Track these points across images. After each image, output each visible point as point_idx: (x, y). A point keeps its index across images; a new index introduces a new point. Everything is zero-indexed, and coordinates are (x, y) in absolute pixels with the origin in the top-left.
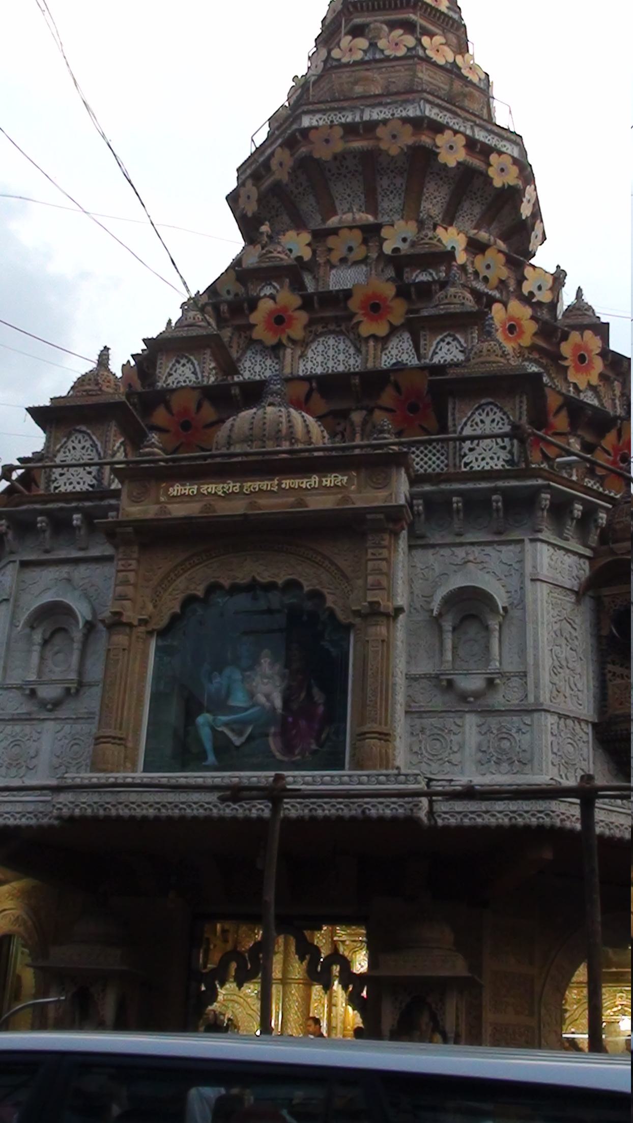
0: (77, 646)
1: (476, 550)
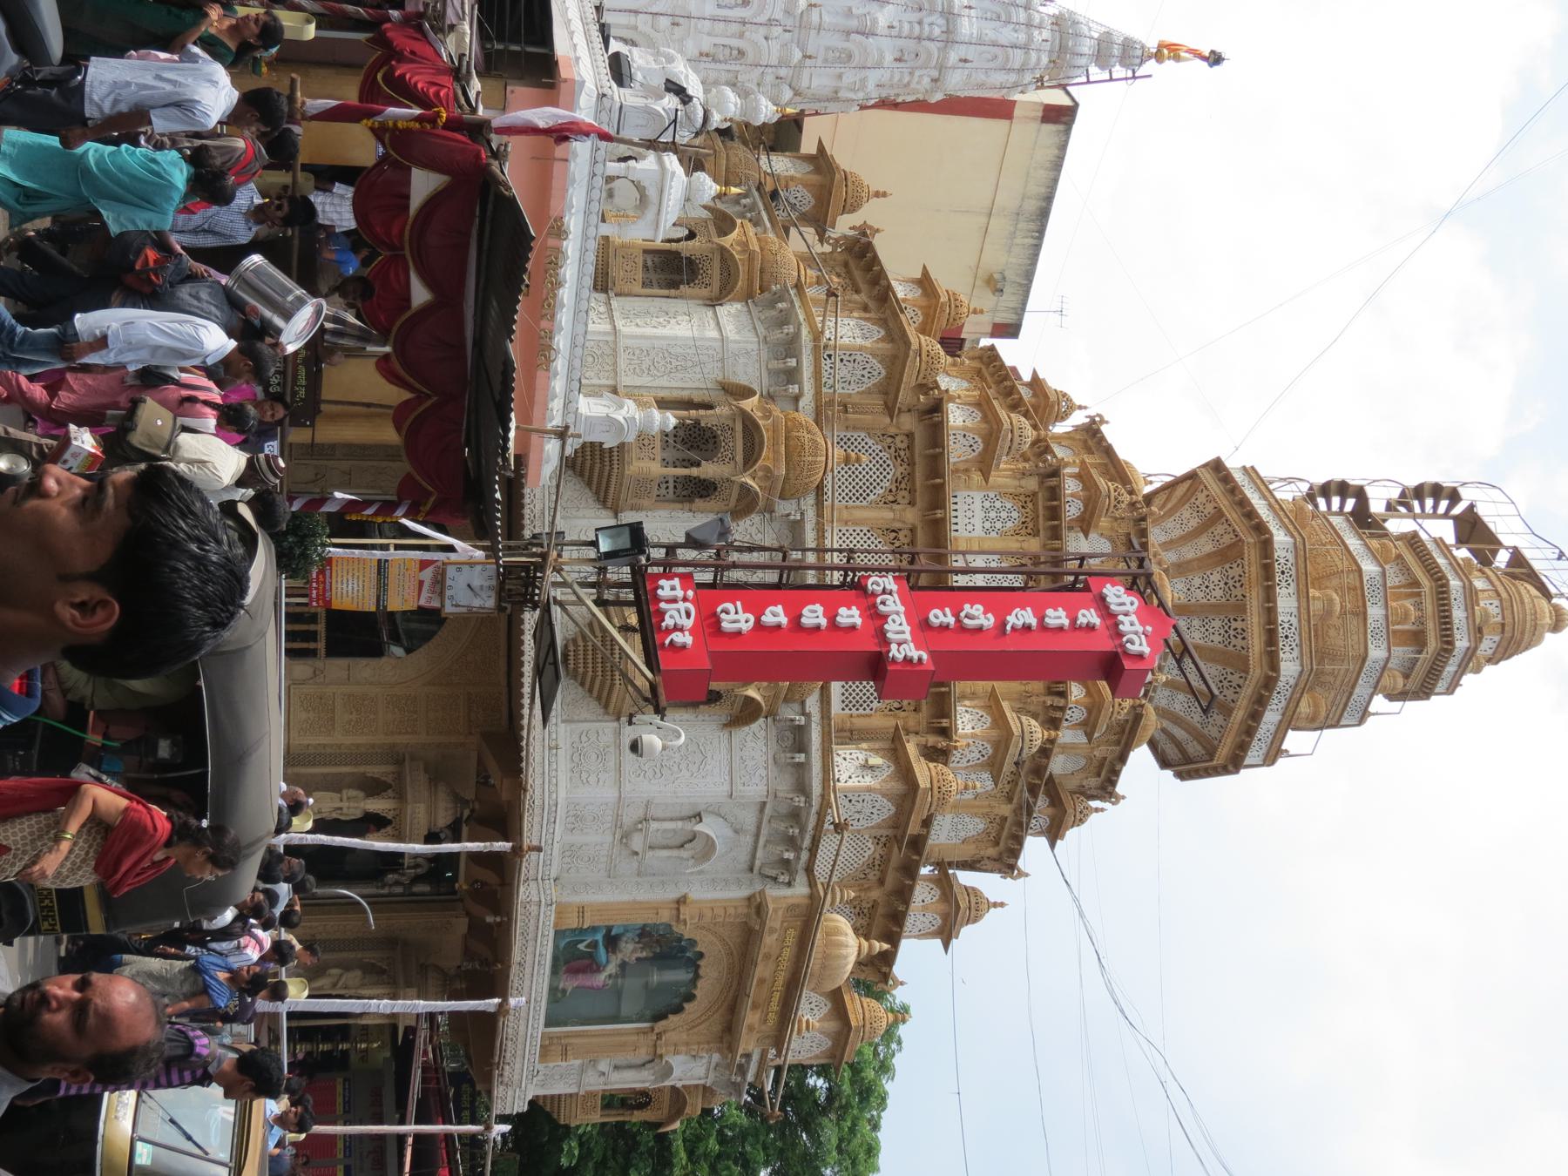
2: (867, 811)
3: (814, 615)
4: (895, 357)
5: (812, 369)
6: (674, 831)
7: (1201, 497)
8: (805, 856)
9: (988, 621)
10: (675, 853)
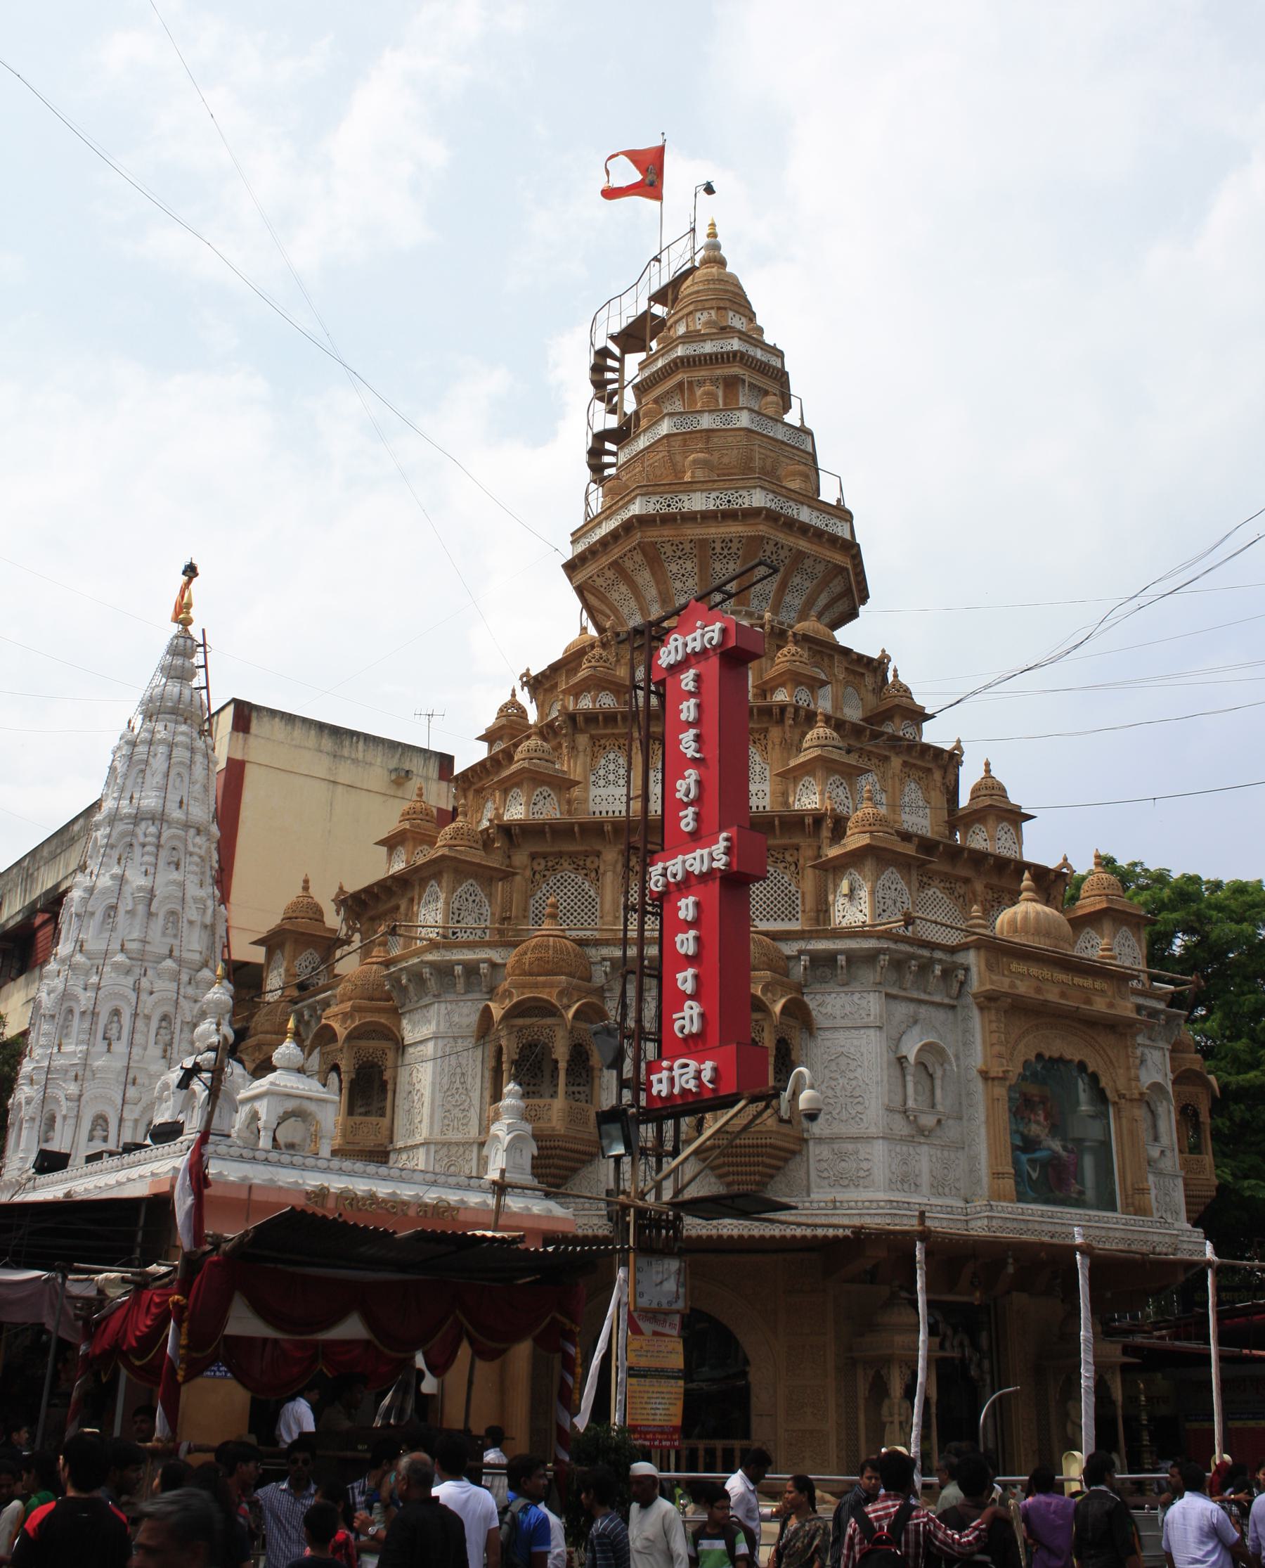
2: (894, 894)
3: (685, 943)
4: (456, 871)
5: (465, 951)
6: (915, 1084)
7: (600, 581)
8: (938, 955)
9: (692, 774)
10: (938, 1083)
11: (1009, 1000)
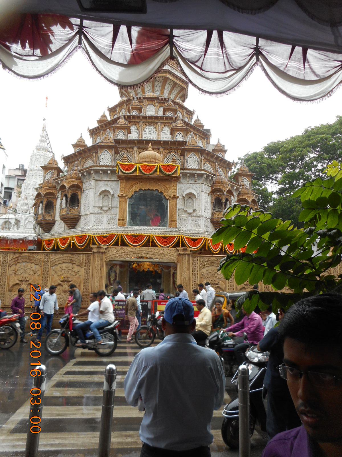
0: (110, 199)
1: (191, 184)
11: (124, 177)
